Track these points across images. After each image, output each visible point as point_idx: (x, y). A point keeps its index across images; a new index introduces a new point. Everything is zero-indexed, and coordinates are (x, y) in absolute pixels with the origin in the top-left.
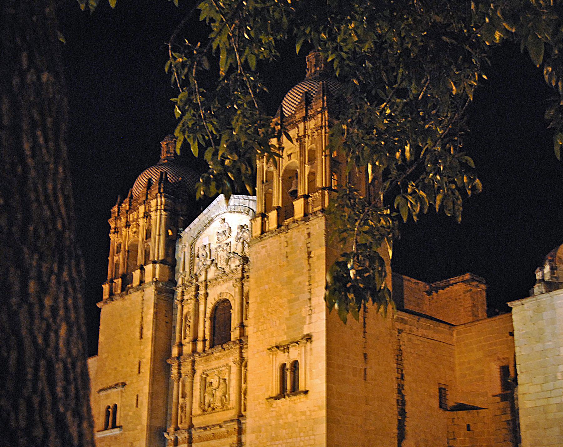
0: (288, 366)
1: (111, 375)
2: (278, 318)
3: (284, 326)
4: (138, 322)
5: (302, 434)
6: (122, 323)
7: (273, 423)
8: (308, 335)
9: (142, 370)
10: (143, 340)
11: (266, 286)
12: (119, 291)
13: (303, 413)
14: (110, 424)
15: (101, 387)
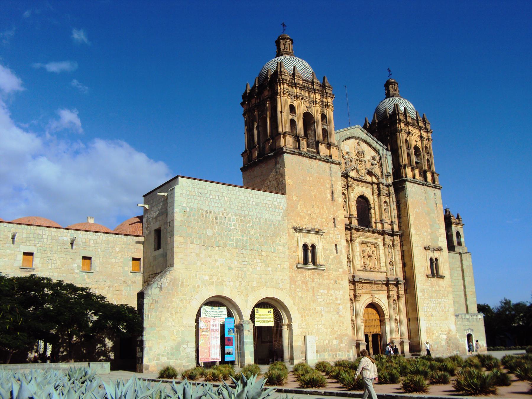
0: (434, 260)
1: (305, 218)
2: (426, 232)
3: (429, 237)
4: (328, 186)
5: (443, 298)
6: (311, 178)
7: (430, 289)
8: (440, 247)
9: (338, 227)
10: (335, 203)
11: (418, 210)
12: (305, 150)
13: (443, 287)
14: (310, 260)
15: (295, 225)
